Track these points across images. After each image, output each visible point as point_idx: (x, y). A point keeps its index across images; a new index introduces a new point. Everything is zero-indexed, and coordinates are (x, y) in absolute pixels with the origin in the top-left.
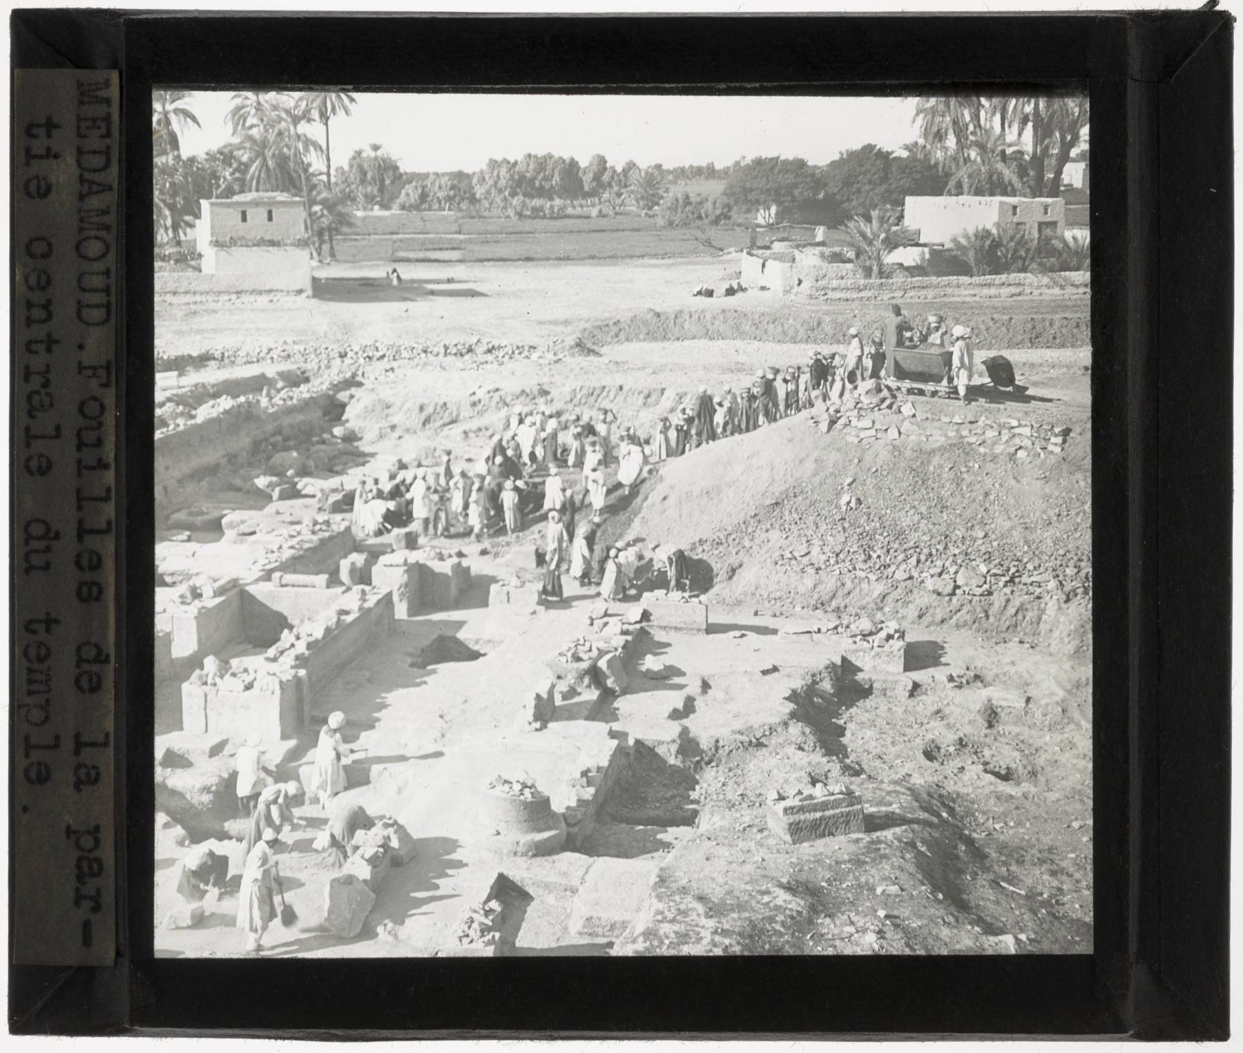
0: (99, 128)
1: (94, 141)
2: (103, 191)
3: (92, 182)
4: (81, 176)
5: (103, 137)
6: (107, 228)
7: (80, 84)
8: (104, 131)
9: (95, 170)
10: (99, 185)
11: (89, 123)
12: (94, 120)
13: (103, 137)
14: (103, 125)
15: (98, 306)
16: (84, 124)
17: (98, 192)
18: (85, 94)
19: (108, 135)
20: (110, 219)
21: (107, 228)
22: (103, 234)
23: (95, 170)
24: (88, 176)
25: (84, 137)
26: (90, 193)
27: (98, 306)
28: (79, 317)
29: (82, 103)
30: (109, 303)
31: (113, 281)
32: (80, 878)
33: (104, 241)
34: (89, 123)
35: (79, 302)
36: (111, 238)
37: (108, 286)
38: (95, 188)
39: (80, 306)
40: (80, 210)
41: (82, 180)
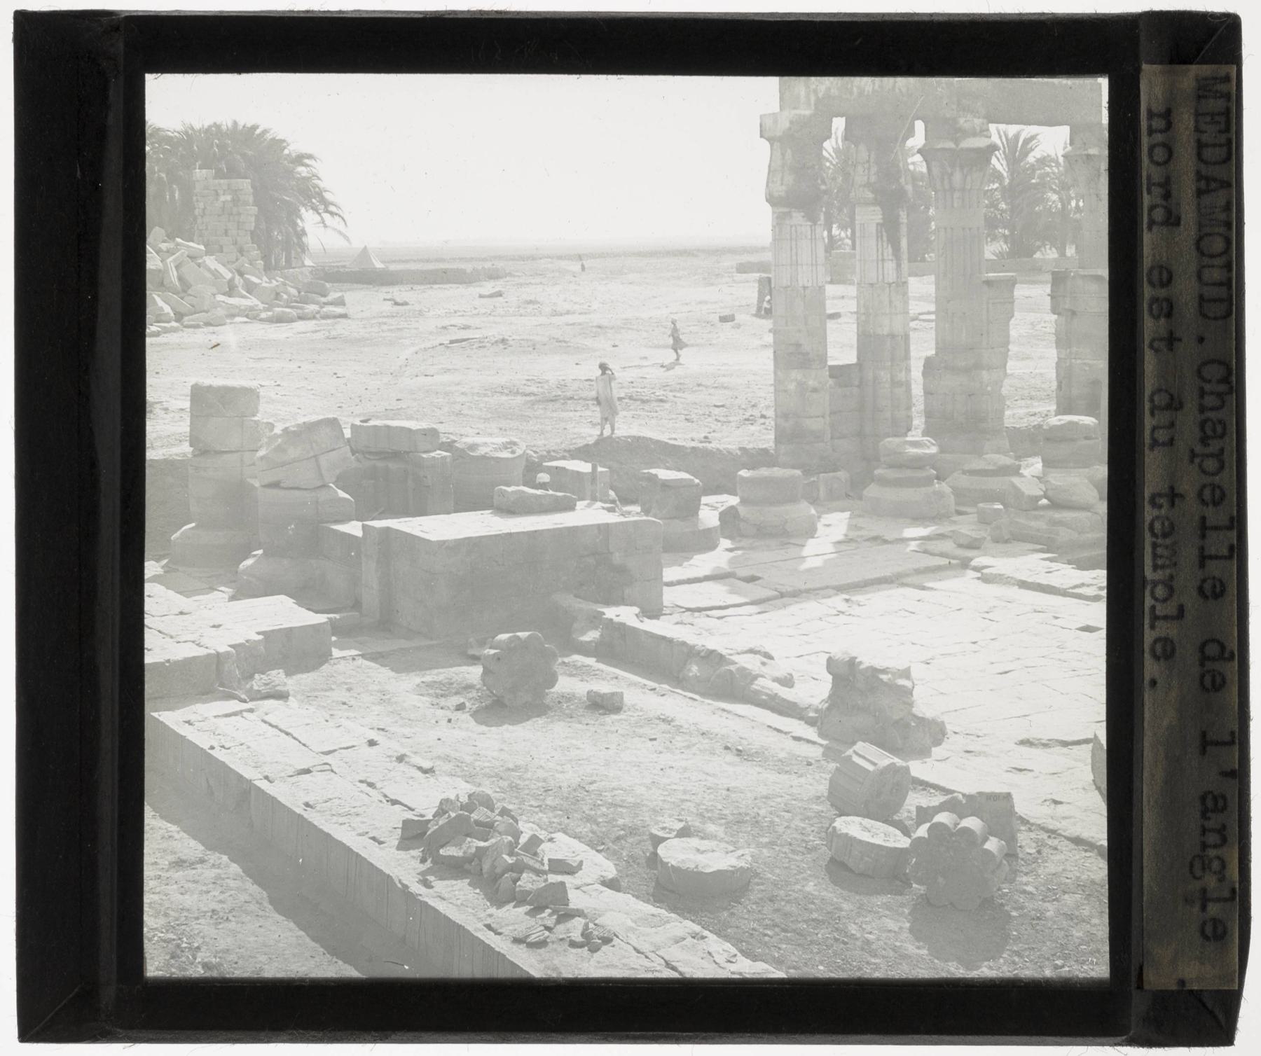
3: (1208, 179)
4: (1198, 173)
5: (1220, 132)
8: (1223, 126)
12: (1213, 115)
13: (1220, 132)
14: (1222, 119)
25: (1202, 132)
32: (1204, 814)
34: (1208, 119)
38: (1213, 185)
41: (1199, 176)
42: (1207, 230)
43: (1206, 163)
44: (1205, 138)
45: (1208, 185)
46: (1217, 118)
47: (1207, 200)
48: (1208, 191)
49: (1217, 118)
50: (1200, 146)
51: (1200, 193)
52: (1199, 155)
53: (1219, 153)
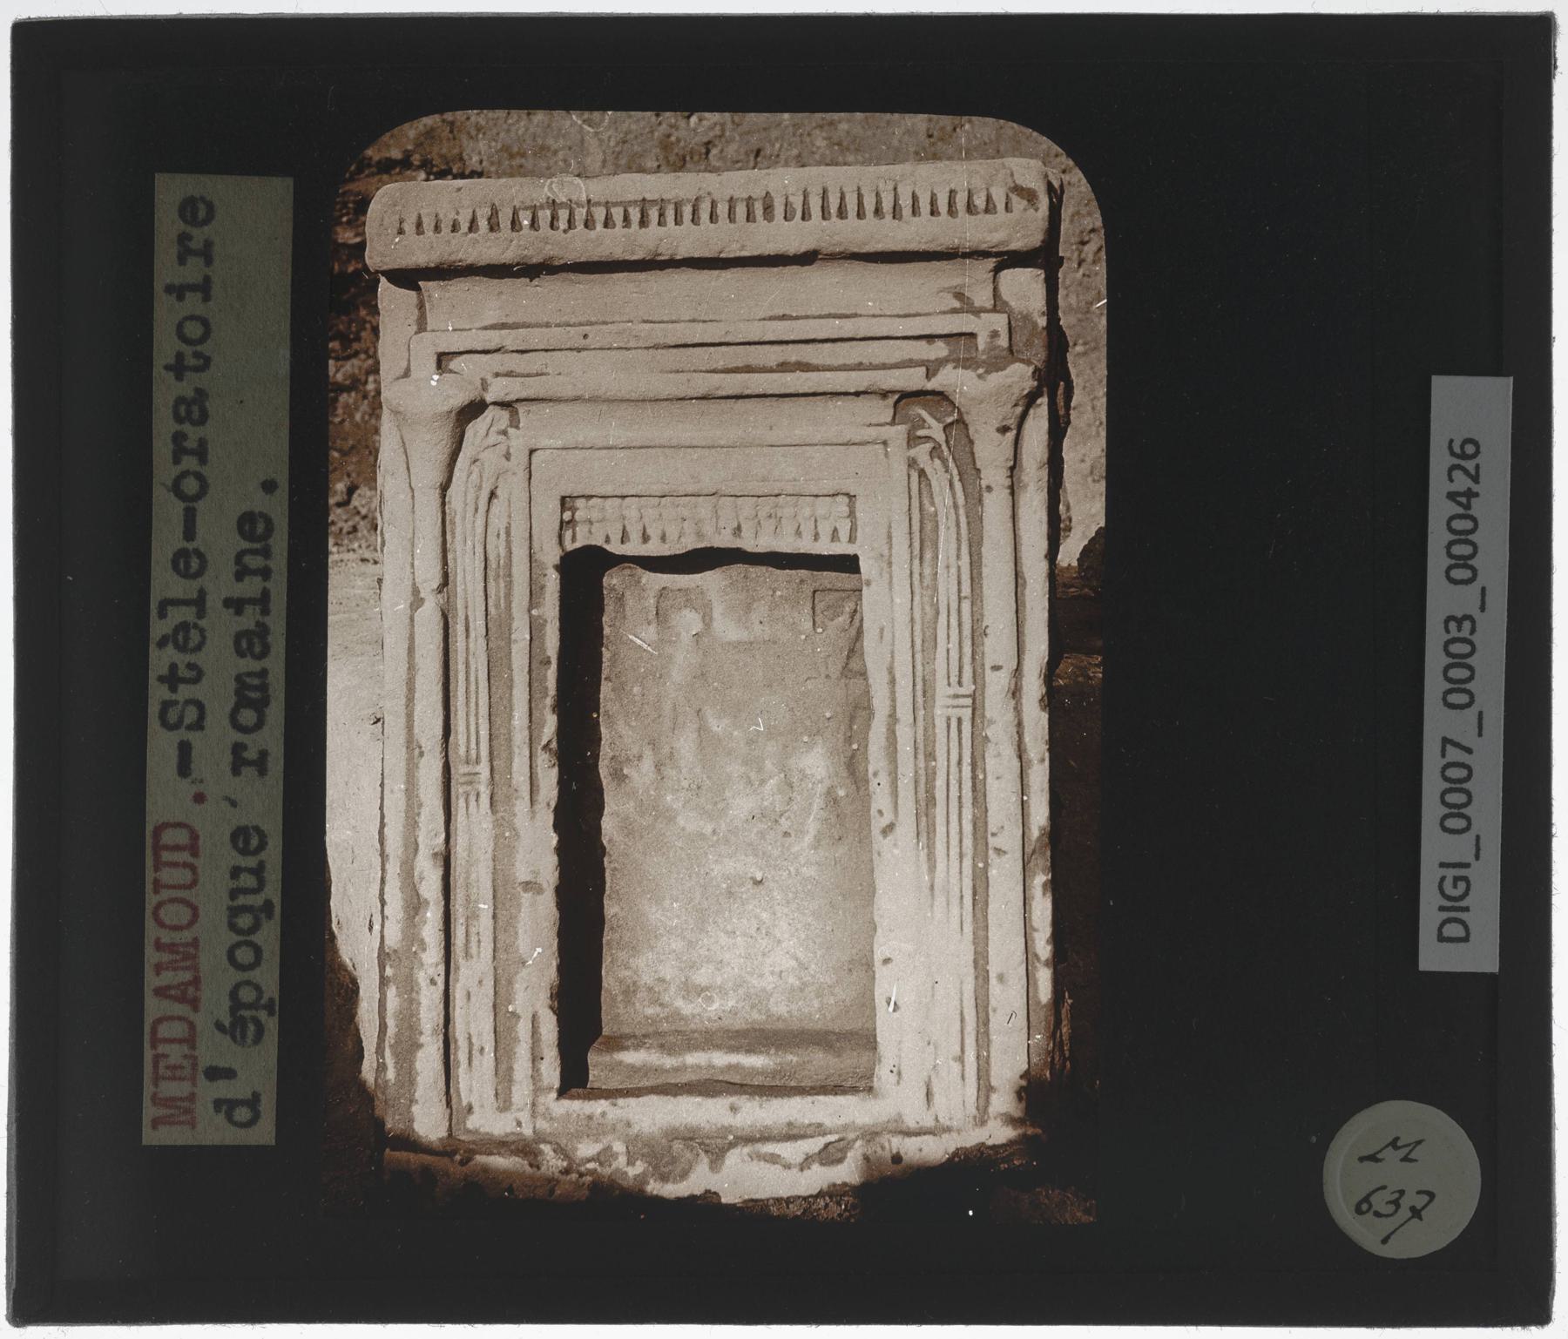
0: (167, 1067)
1: (175, 1053)
2: (168, 987)
6: (159, 946)
7: (193, 1124)
8: (162, 1064)
9: (172, 1018)
10: (170, 997)
12: (174, 1078)
13: (166, 1056)
14: (161, 1071)
16: (187, 1072)
18: (183, 1110)
19: (157, 1058)
20: (151, 956)
21: (159, 946)
22: (166, 937)
23: (172, 1018)
25: (185, 1056)
29: (192, 1097)
31: (150, 875)
33: (161, 924)
34: (178, 1073)
35: (195, 854)
36: (151, 931)
37: (157, 869)
39: (193, 849)
42: (186, 936)
43: (180, 1018)
44: (185, 1049)
46: (169, 1073)
49: (169, 1073)
50: (190, 1040)
52: (192, 1026)
53: (164, 1031)
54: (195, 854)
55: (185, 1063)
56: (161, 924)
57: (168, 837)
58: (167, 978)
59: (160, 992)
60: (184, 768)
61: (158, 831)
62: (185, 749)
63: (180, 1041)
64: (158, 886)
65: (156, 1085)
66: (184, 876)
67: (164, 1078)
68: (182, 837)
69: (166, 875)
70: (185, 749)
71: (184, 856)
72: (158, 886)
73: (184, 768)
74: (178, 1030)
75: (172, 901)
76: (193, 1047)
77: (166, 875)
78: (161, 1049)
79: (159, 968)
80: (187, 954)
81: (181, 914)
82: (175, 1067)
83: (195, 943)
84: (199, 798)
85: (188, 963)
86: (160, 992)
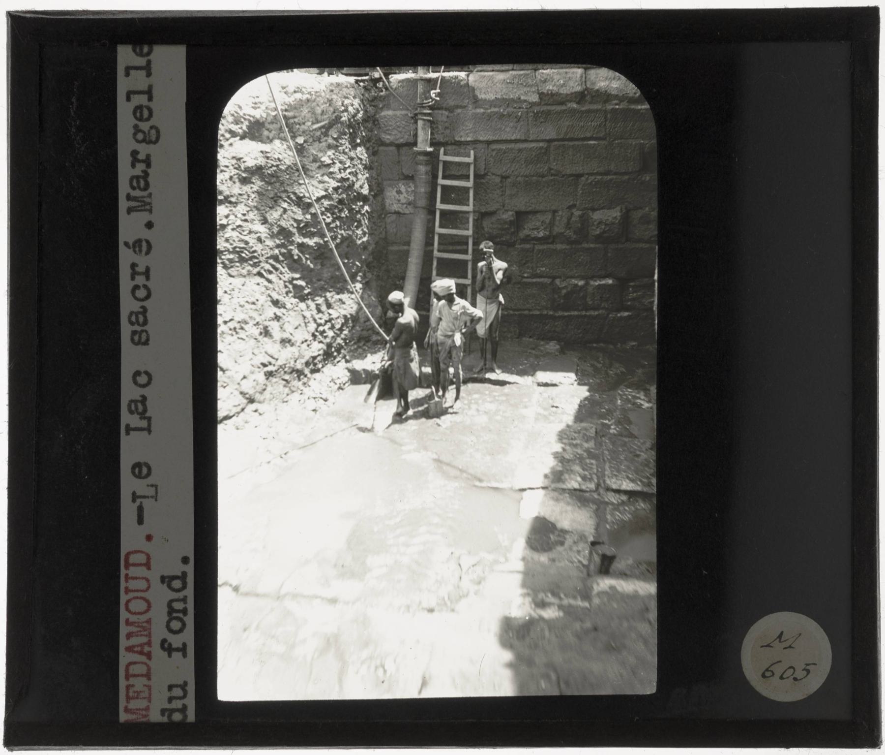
0: (134, 692)
1: (139, 684)
2: (133, 646)
3: (141, 653)
5: (133, 686)
6: (127, 622)
8: (131, 691)
10: (137, 652)
11: (143, 695)
13: (133, 686)
14: (131, 694)
15: (135, 565)
16: (146, 695)
17: (138, 646)
19: (128, 687)
24: (143, 659)
25: (145, 685)
26: (142, 645)
27: (135, 565)
28: (148, 557)
30: (127, 567)
34: (143, 695)
35: (149, 568)
36: (124, 615)
38: (139, 649)
39: (148, 565)
40: (149, 635)
41: (149, 656)
43: (142, 663)
44: (144, 680)
45: (143, 648)
47: (144, 640)
48: (145, 644)
50: (148, 676)
51: (149, 644)
53: (134, 669)
54: (149, 568)
55: (146, 689)
56: (127, 609)
57: (133, 559)
58: (134, 641)
59: (129, 649)
60: (140, 521)
61: (128, 555)
62: (140, 509)
63: (142, 675)
64: (127, 590)
65: (128, 702)
66: (143, 585)
67: (133, 698)
68: (141, 558)
69: (132, 584)
70: (140, 509)
71: (141, 571)
72: (127, 590)
73: (140, 521)
74: (142, 669)
75: (137, 598)
76: (149, 679)
77: (132, 584)
78: (132, 681)
79: (129, 636)
80: (146, 628)
81: (143, 606)
82: (138, 692)
83: (149, 621)
84: (149, 538)
85: (145, 633)
86: (129, 649)
